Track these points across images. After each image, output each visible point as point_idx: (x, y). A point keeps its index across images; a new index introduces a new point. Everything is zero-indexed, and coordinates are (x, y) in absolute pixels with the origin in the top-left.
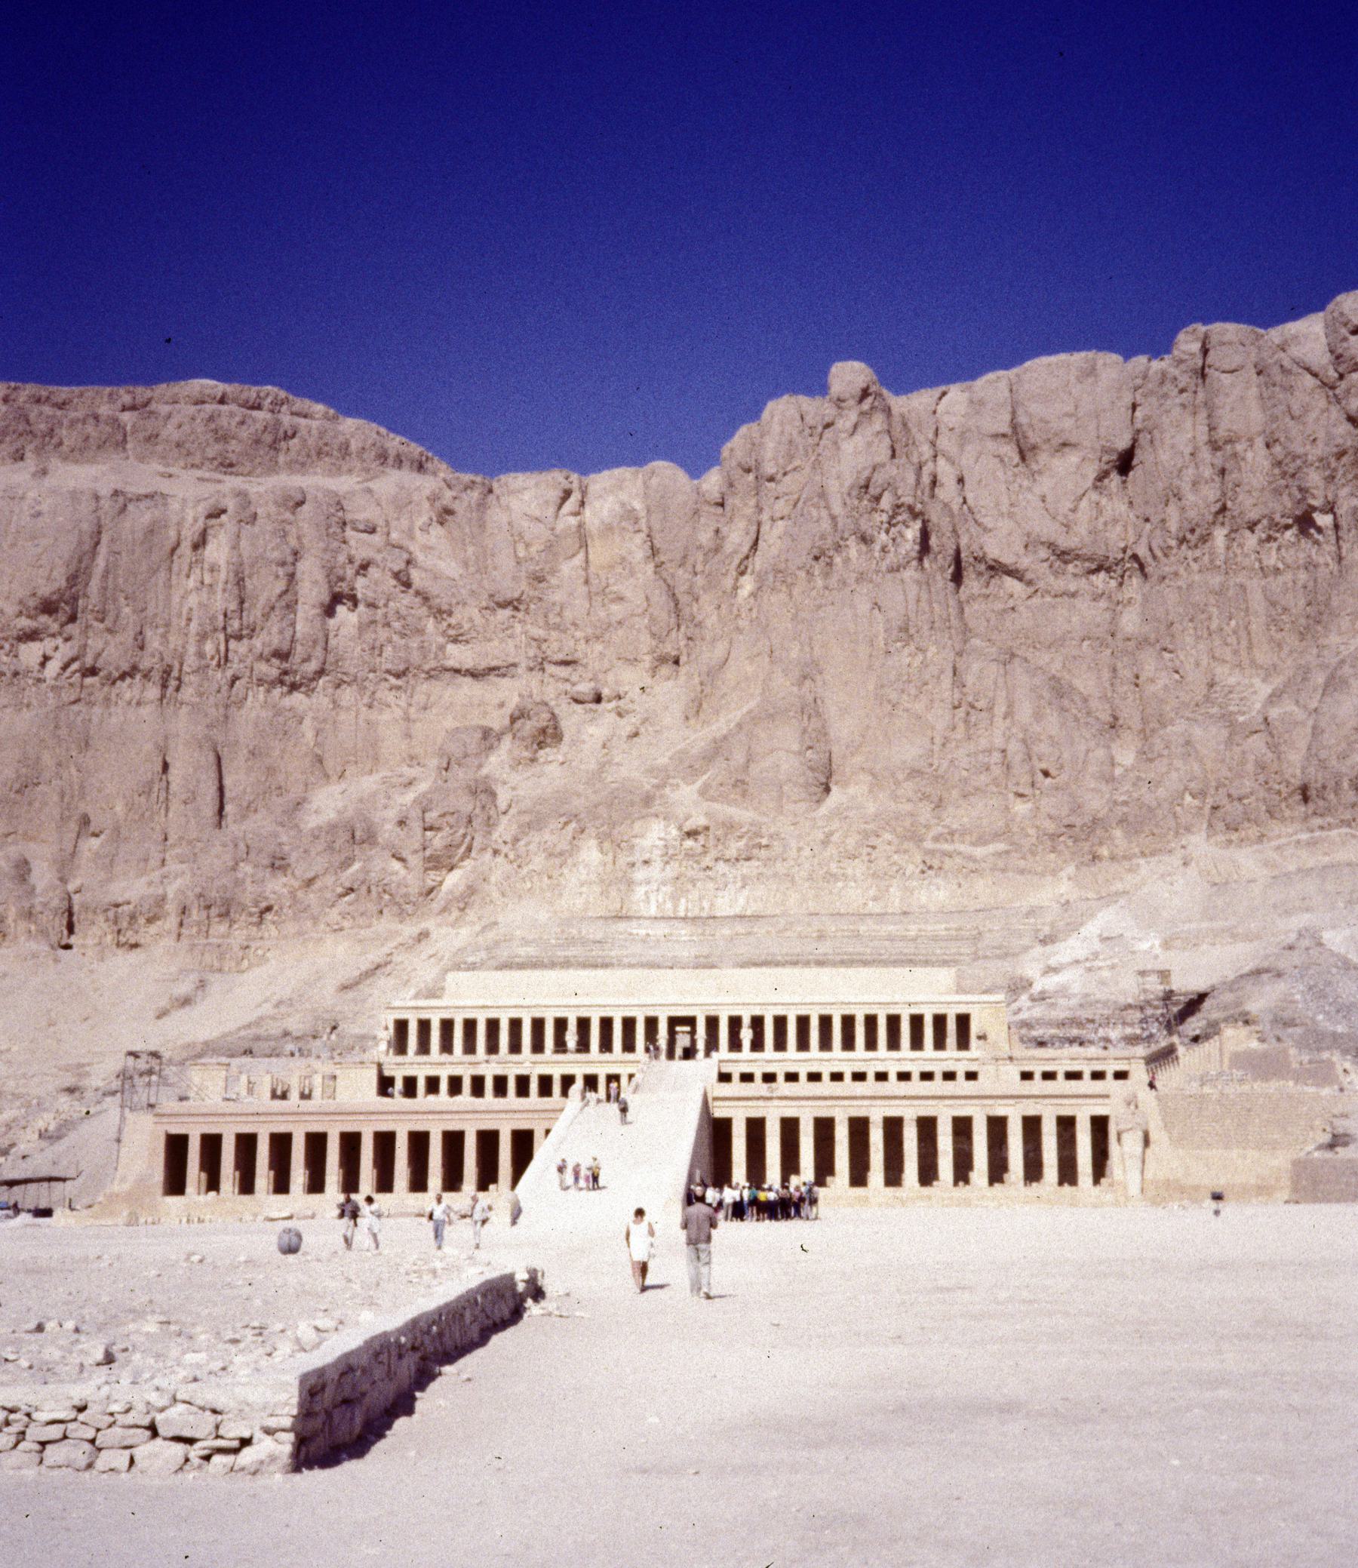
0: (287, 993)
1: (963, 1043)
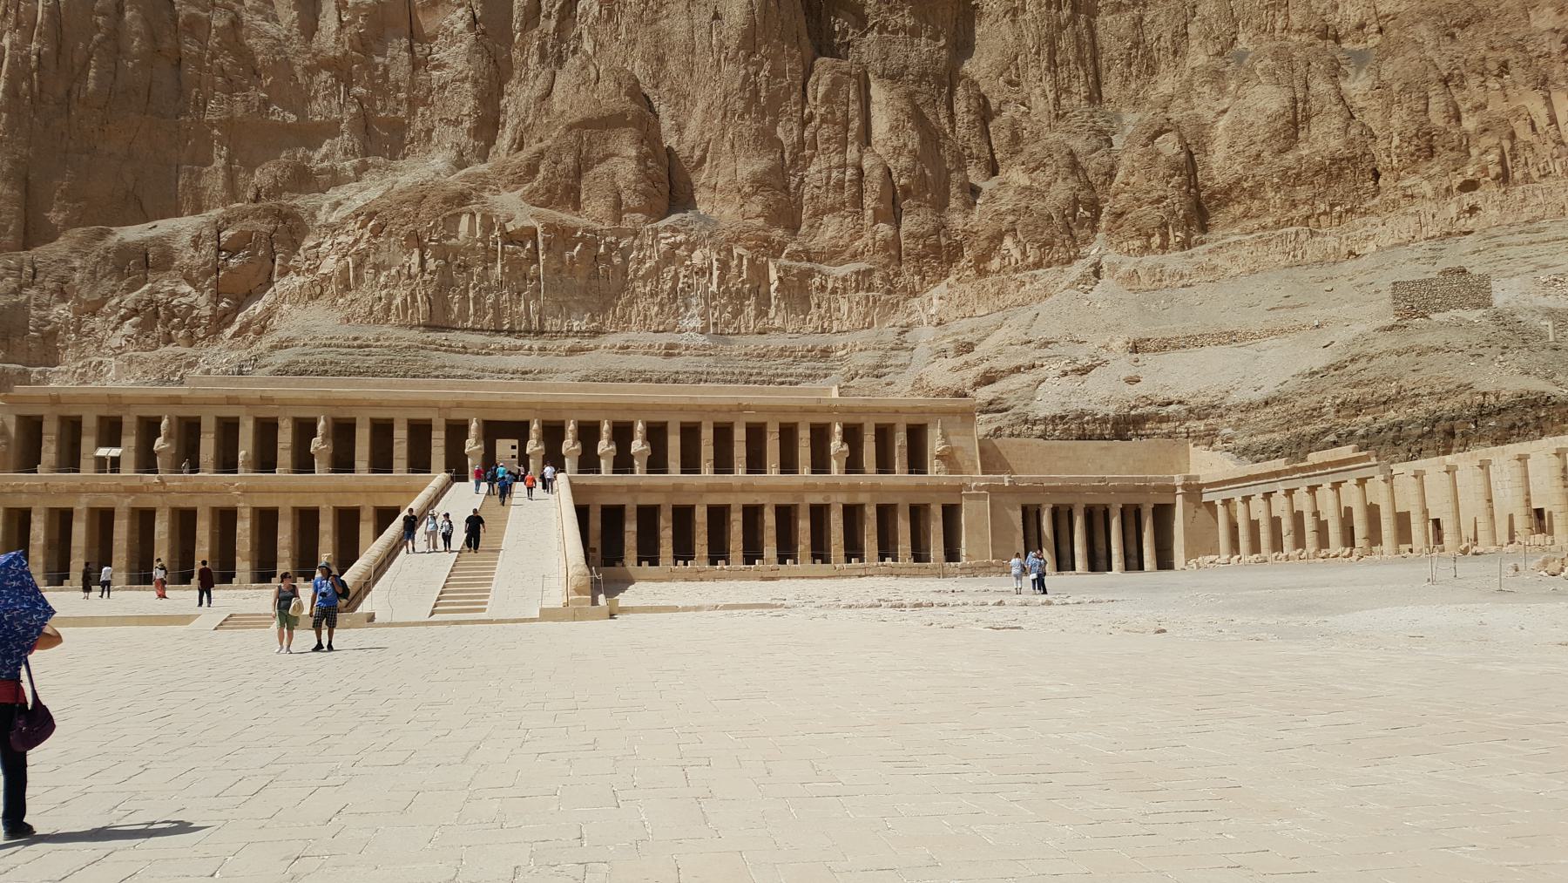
1: (917, 463)
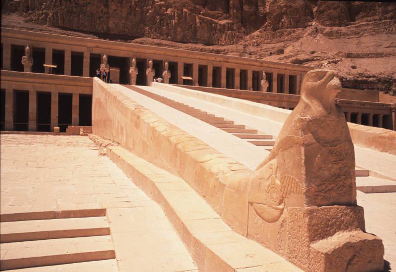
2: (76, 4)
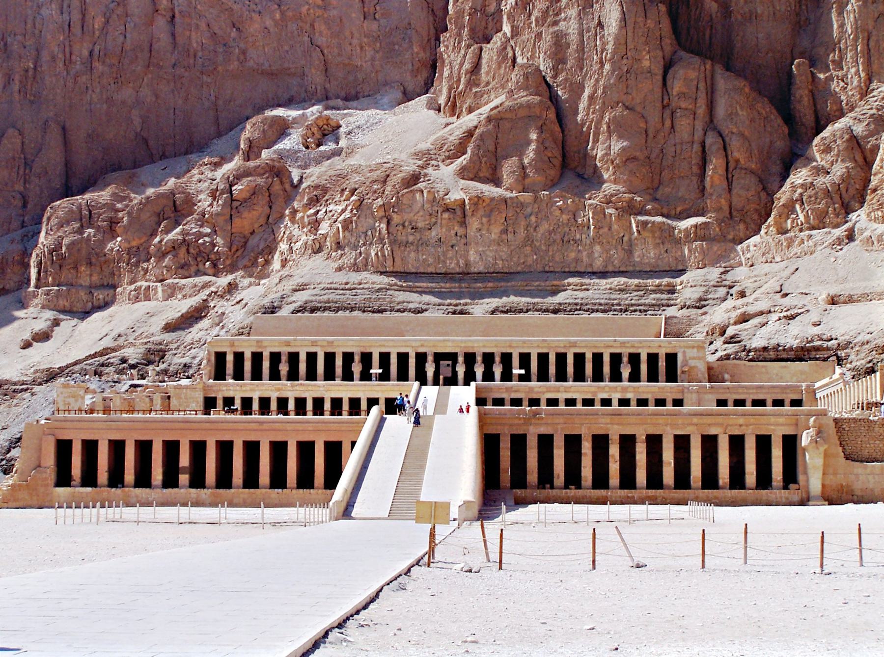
0: (121, 329)
2: (413, 228)
